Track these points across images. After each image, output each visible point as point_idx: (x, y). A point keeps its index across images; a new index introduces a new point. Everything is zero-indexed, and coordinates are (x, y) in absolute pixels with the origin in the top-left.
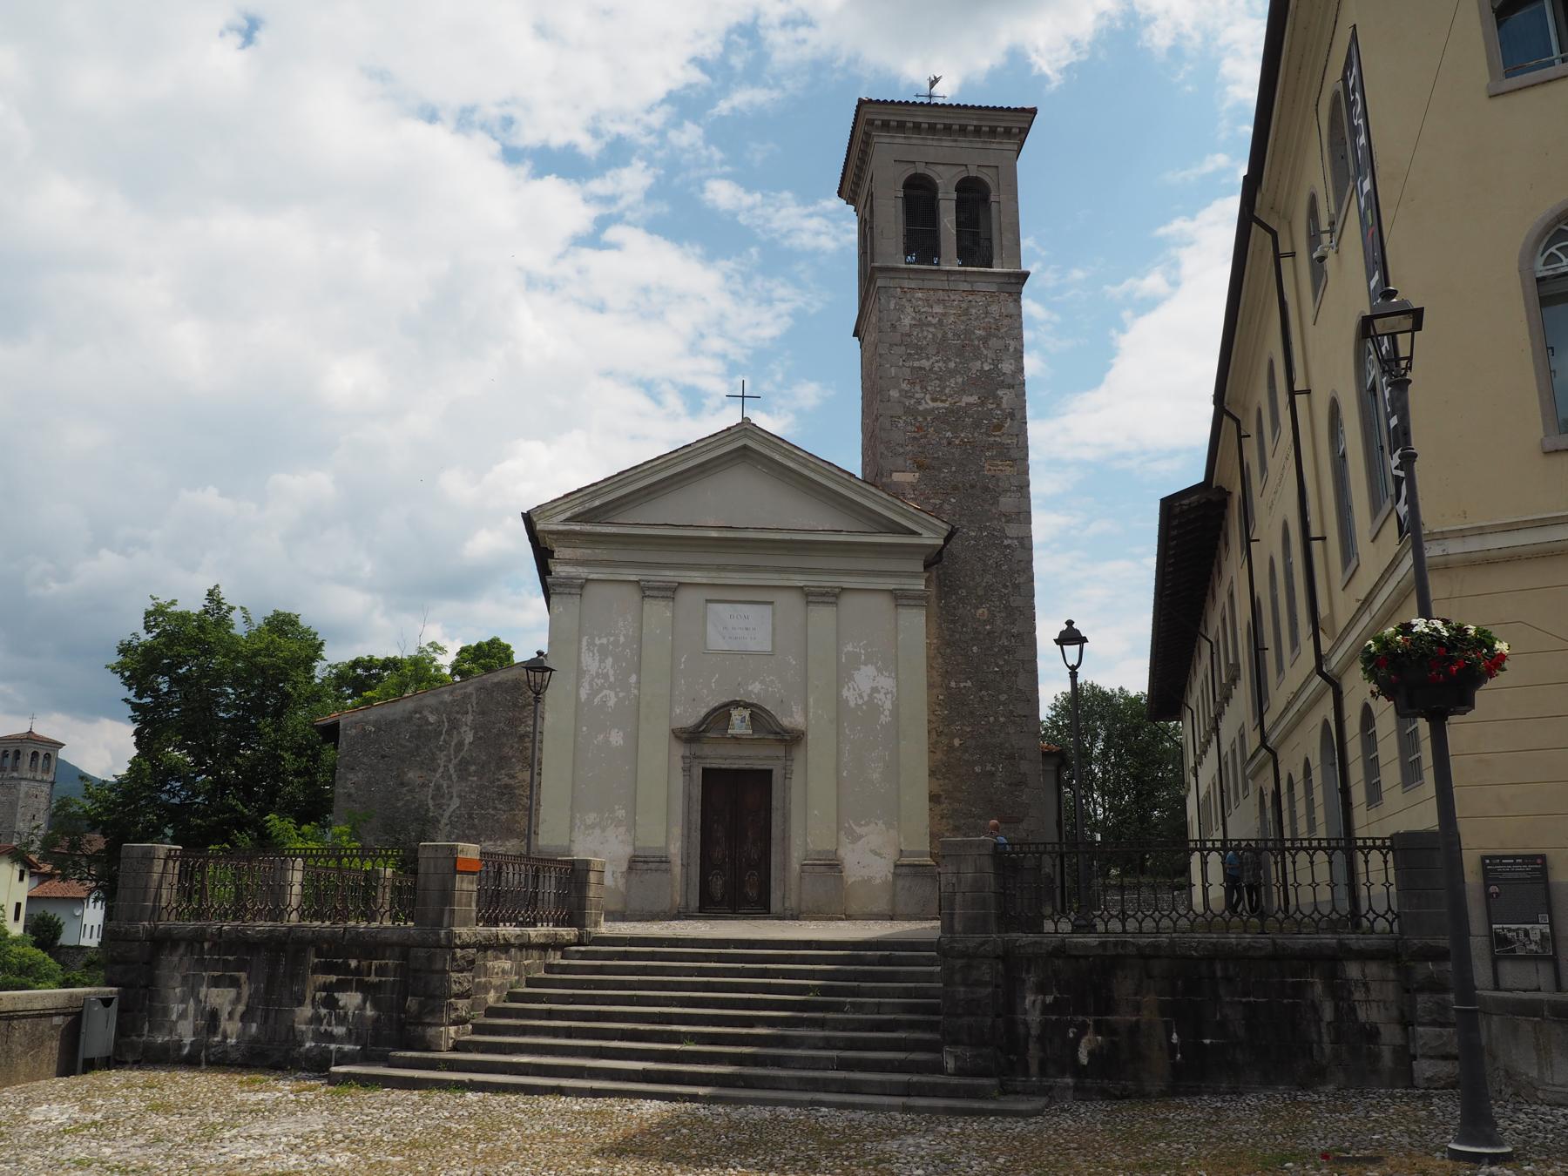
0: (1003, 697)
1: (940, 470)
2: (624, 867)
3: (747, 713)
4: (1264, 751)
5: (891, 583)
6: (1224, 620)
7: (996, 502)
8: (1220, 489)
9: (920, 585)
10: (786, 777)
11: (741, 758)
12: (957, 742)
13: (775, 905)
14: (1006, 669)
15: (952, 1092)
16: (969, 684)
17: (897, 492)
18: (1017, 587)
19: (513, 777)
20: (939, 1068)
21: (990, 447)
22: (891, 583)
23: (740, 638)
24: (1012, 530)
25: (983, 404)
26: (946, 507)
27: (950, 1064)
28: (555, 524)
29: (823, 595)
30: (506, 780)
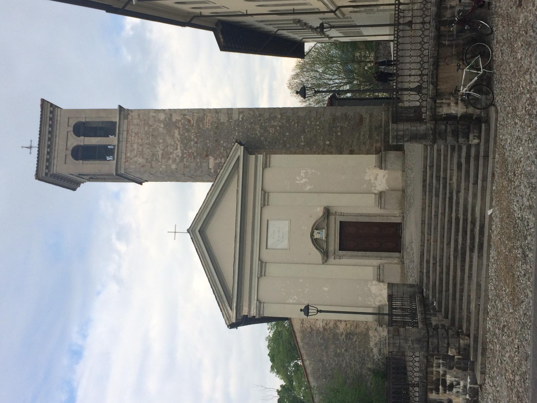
0: (308, 122)
1: (208, 147)
2: (382, 284)
3: (316, 232)
4: (337, 12)
5: (260, 169)
6: (270, 24)
7: (223, 123)
8: (217, 24)
9: (261, 157)
10: (342, 214)
11: (335, 234)
12: (328, 143)
13: (398, 220)
14: (296, 121)
15: (487, 141)
16: (302, 137)
17: (219, 166)
18: (260, 115)
19: (342, 334)
20: (478, 145)
21: (198, 125)
22: (260, 169)
23: (285, 232)
24: (235, 116)
25: (179, 128)
26: (225, 145)
27: (476, 141)
28: (233, 315)
29: (264, 199)
30: (343, 336)
